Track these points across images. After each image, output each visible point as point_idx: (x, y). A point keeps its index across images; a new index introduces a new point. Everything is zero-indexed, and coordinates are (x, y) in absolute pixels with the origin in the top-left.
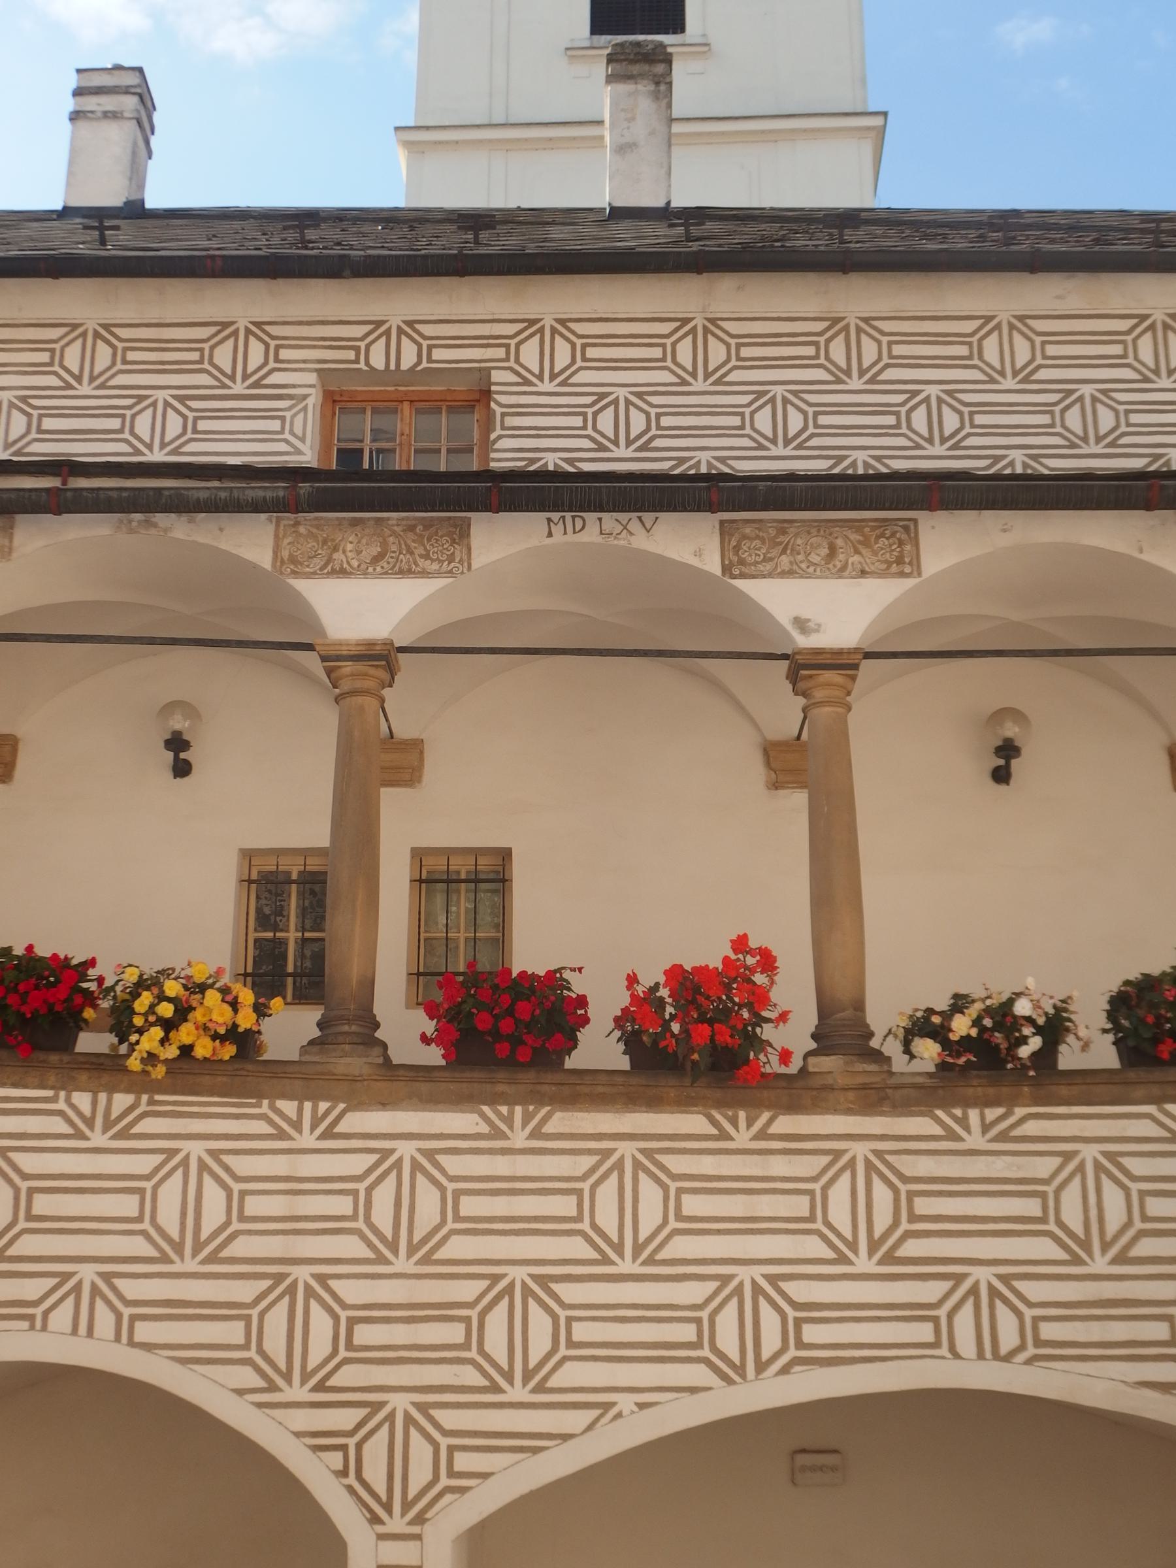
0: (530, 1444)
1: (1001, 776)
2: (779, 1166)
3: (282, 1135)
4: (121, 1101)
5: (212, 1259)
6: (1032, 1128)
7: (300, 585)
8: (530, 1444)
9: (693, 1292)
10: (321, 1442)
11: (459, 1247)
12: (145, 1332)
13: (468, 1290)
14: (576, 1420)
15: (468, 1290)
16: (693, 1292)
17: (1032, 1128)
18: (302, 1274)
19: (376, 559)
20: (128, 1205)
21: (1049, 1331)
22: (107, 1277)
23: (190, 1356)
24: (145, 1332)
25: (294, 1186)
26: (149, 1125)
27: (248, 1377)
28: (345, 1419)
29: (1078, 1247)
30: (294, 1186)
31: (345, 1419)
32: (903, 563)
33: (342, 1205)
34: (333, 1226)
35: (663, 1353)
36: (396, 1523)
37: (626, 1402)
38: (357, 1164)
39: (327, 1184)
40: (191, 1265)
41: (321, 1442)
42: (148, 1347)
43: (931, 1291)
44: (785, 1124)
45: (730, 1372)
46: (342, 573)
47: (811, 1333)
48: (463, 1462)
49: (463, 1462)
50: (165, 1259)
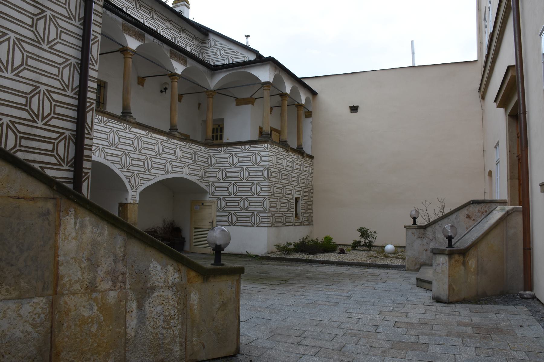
0: (148, 180)
1: (162, 92)
2: (172, 146)
3: (124, 130)
4: (105, 119)
5: (116, 147)
6: (191, 146)
7: (125, 35)
8: (148, 180)
9: (164, 162)
10: (128, 177)
11: (143, 151)
12: (108, 158)
13: (143, 157)
14: (152, 177)
15: (143, 157)
16: (164, 162)
17: (191, 146)
18: (126, 152)
19: (134, 35)
20: (105, 136)
21: (191, 172)
22: (103, 148)
23: (113, 162)
24: (108, 158)
25: (126, 138)
26: (108, 124)
27: (119, 166)
28: (130, 174)
29: (194, 161)
30: (126, 138)
31: (130, 174)
32: (184, 63)
33: (131, 142)
34: (130, 145)
35: (161, 169)
36: (134, 190)
37: (157, 175)
38: (133, 136)
39: (130, 139)
40: (113, 148)
41: (128, 177)
42: (108, 160)
43: (183, 165)
44: (173, 141)
45: (167, 173)
46: (130, 35)
47: (174, 169)
48: (142, 182)
49: (142, 182)
50: (110, 146)
